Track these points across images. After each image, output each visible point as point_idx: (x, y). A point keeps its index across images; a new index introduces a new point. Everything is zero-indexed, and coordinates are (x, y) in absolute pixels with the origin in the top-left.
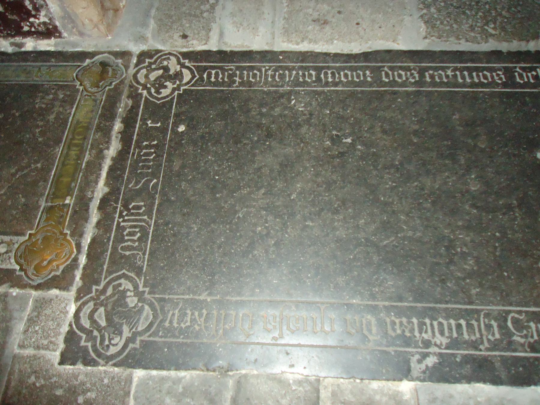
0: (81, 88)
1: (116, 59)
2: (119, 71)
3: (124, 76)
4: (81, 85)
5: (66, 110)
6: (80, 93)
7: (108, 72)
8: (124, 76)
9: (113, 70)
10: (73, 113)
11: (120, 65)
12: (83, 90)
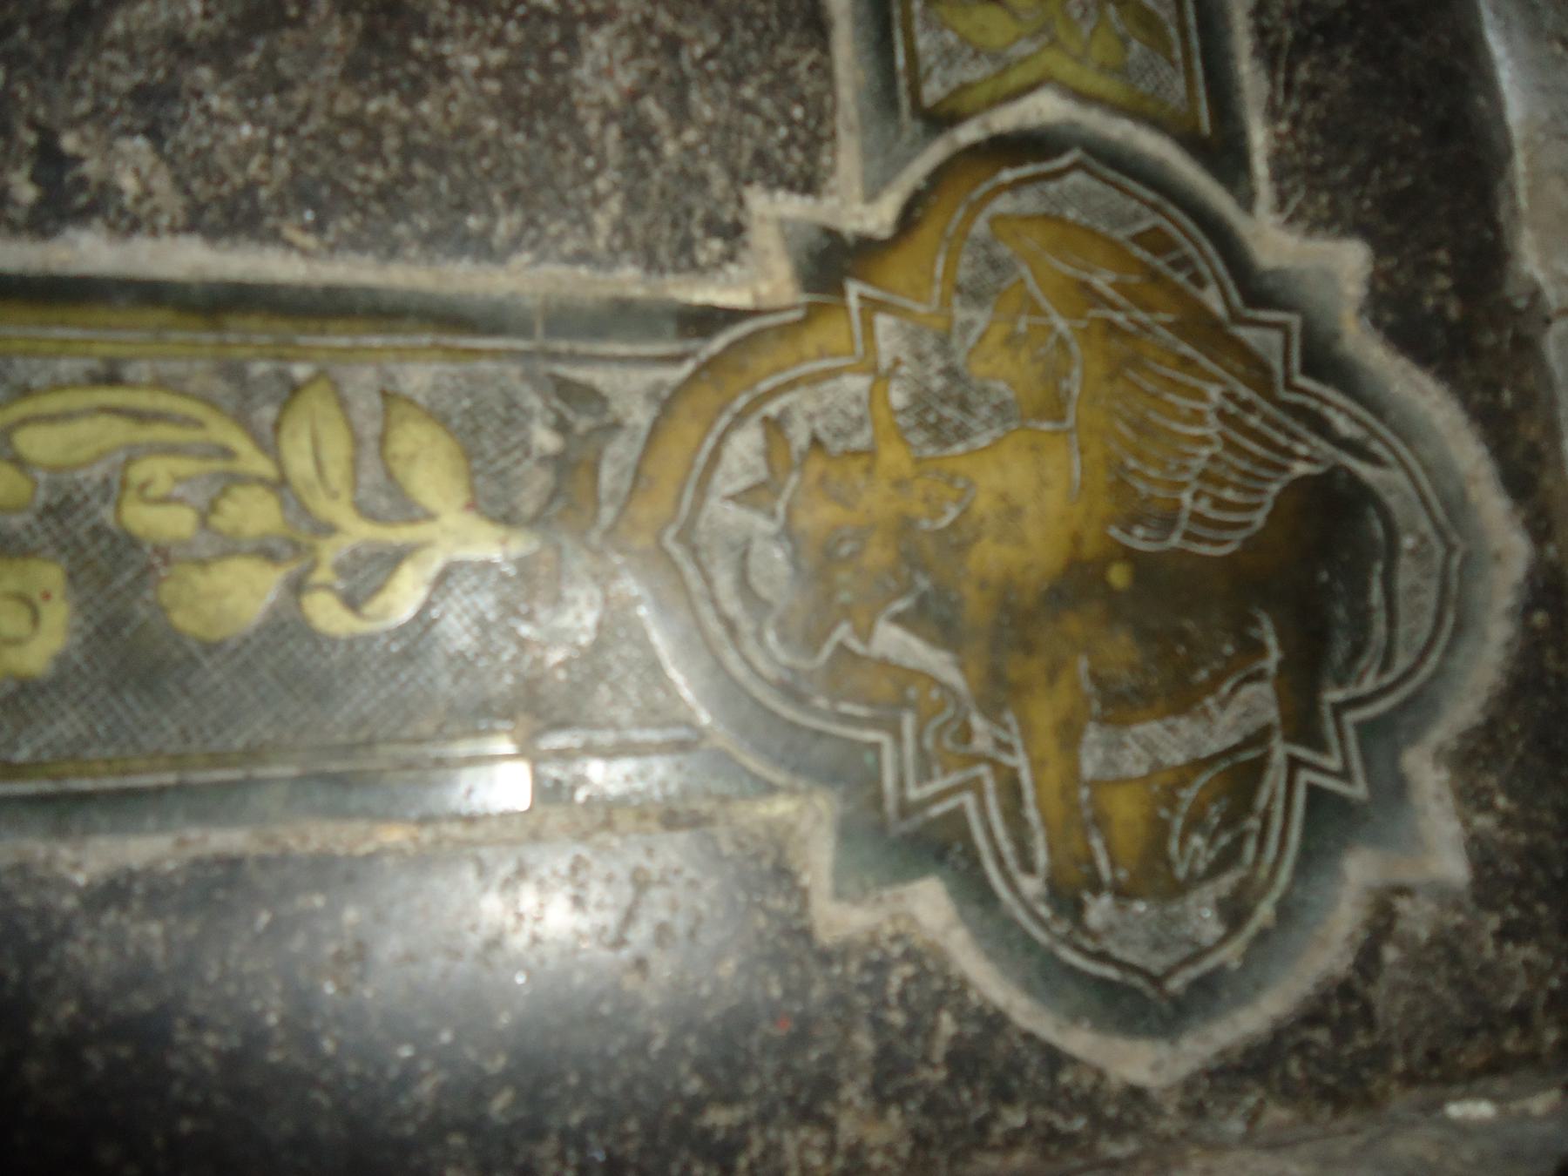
0: (760, 280)
1: (1471, 758)
2: (1234, 913)
3: (1136, 1062)
4: (831, 262)
5: (154, 108)
6: (629, 280)
7: (1182, 698)
8: (1136, 1062)
9: (1240, 774)
10: (88, 251)
11: (1360, 869)
12: (706, 320)
